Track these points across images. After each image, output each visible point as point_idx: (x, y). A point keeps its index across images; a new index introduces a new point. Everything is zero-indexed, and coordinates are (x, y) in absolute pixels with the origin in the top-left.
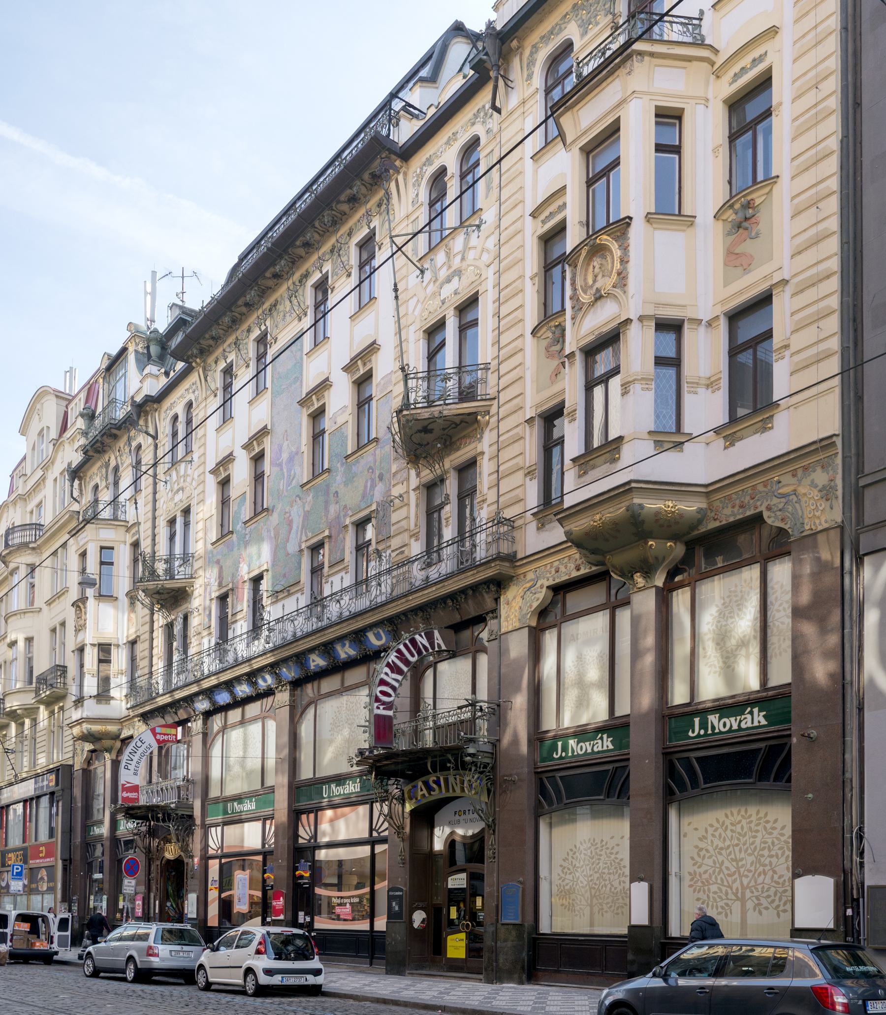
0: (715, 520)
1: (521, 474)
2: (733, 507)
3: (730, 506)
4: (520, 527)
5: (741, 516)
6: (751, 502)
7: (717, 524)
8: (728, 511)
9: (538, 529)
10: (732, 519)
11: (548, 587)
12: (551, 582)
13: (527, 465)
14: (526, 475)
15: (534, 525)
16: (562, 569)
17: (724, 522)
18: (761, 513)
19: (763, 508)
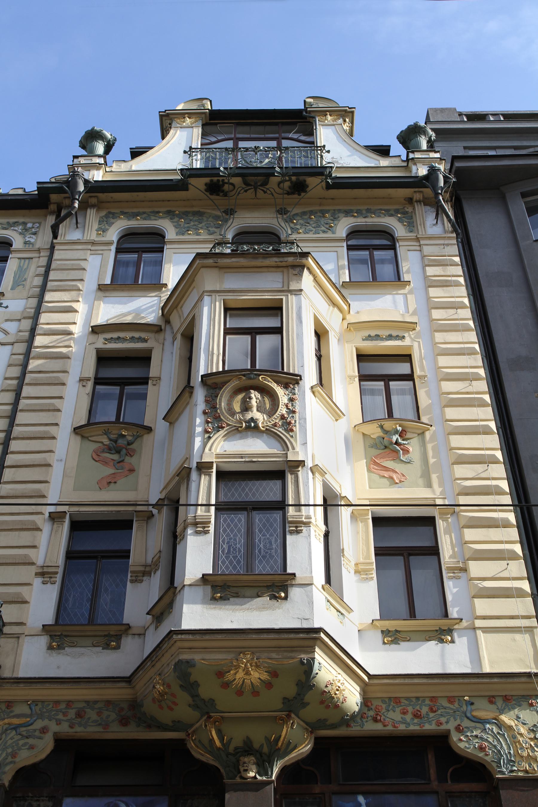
0: (375, 720)
1: (33, 570)
2: (404, 713)
3: (398, 710)
4: (17, 637)
5: (417, 728)
6: (431, 715)
7: (379, 727)
8: (395, 715)
9: (50, 648)
10: (402, 727)
11: (55, 734)
12: (64, 729)
13: (40, 562)
14: (37, 574)
15: (44, 640)
16: (92, 714)
17: (390, 728)
18: (449, 731)
19: (451, 726)
